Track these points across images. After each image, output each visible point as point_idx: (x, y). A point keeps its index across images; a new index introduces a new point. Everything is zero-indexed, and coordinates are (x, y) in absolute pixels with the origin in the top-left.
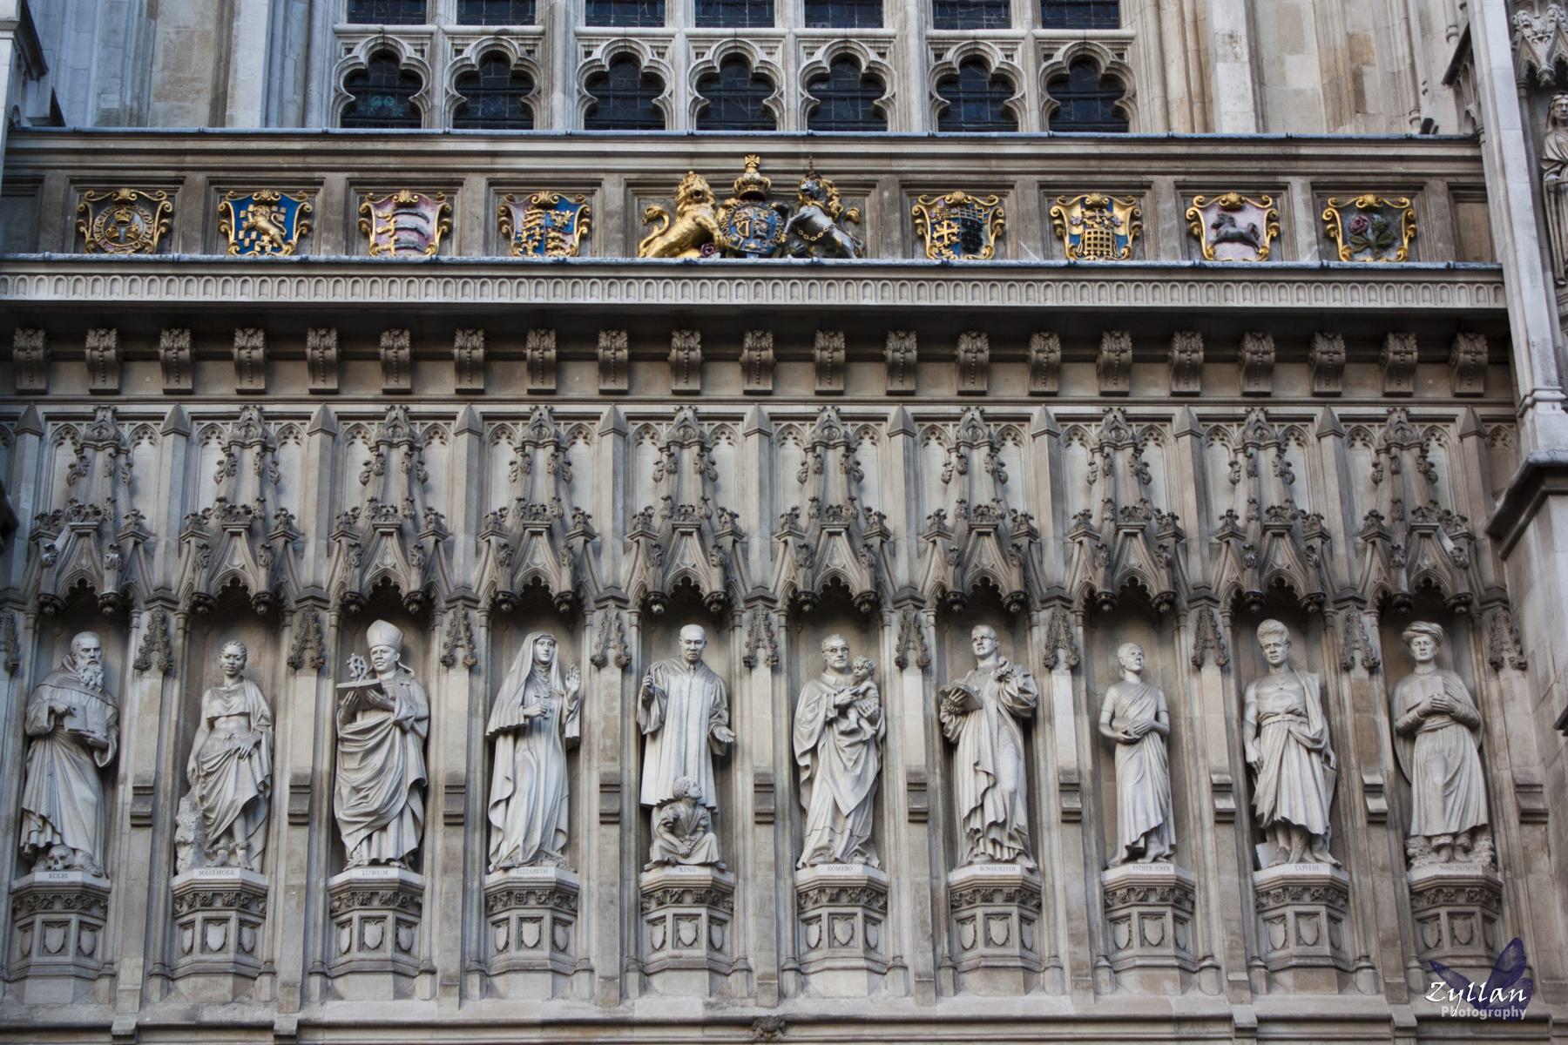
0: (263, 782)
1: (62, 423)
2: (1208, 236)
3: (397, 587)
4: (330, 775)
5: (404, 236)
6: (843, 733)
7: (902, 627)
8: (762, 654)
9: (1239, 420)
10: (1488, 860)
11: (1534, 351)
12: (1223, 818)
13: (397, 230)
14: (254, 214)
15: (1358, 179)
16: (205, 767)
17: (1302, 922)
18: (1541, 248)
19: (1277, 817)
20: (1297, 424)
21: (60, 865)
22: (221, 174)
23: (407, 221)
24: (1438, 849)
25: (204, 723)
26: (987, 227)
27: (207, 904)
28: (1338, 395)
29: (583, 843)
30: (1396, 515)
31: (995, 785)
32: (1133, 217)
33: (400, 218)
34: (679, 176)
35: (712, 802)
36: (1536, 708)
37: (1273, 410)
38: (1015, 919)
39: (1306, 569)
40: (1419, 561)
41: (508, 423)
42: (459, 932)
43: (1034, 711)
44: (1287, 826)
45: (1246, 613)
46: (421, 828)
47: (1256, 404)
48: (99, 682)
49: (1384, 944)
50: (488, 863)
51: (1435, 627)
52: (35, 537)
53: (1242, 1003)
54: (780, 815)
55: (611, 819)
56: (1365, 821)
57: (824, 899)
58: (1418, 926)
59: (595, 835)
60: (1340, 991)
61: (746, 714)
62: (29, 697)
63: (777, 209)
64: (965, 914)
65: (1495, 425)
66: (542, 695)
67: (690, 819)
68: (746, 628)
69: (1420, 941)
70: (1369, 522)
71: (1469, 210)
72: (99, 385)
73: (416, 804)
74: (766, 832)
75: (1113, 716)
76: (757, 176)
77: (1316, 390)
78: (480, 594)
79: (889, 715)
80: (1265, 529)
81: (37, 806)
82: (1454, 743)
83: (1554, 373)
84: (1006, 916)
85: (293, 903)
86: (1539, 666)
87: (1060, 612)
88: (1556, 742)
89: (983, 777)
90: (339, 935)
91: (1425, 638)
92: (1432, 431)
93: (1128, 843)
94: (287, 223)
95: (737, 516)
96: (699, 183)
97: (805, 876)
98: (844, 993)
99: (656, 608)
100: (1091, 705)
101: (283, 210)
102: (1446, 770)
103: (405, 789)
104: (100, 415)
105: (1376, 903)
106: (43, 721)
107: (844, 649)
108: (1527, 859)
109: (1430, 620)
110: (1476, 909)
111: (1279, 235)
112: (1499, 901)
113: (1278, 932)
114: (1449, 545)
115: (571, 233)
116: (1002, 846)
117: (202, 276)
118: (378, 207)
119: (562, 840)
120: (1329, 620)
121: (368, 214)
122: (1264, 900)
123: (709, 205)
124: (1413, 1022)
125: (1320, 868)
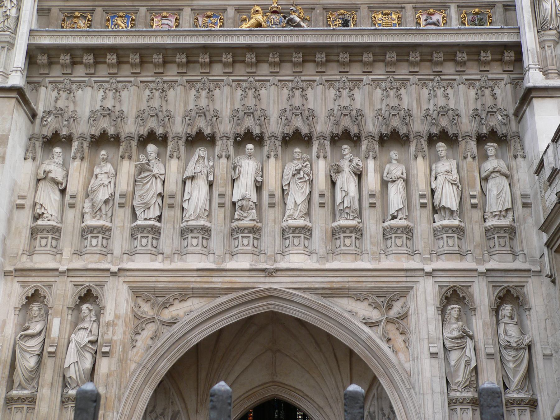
0: (111, 194)
1: (54, 84)
2: (423, 23)
3: (155, 133)
4: (133, 192)
5: (164, 26)
6: (298, 179)
7: (319, 145)
8: (272, 154)
9: (432, 80)
10: (512, 219)
11: (529, 52)
12: (423, 206)
13: (161, 24)
14: (117, 20)
15: (473, 4)
16: (93, 189)
17: (449, 239)
18: (533, 20)
19: (441, 206)
20: (451, 81)
21: (46, 219)
22: (106, 8)
23: (165, 22)
24: (495, 216)
25: (94, 176)
26: (351, 21)
27: (92, 232)
28: (464, 71)
29: (213, 214)
30: (483, 109)
31: (347, 195)
32: (398, 18)
33: (163, 21)
34: (252, 6)
35: (255, 201)
36: (528, 170)
37: (443, 77)
38: (354, 238)
39: (452, 126)
40: (490, 123)
41: (194, 83)
42: (171, 241)
43: (362, 172)
44: (444, 208)
45: (432, 140)
46: (161, 209)
47: (436, 75)
48: (61, 163)
49: (475, 246)
50: (182, 220)
51: (495, 145)
52: (42, 118)
53: (427, 265)
54: (276, 204)
55: (222, 206)
56: (470, 207)
57: (291, 231)
58: (488, 241)
59: (217, 211)
60: (461, 261)
61: (267, 173)
62: (39, 167)
63: (283, 16)
64: (337, 237)
65: (517, 81)
66: (200, 166)
67: (247, 206)
68: (268, 146)
69: (488, 246)
70: (474, 111)
71: (510, 14)
72: (65, 72)
73: (160, 200)
74: (271, 211)
75: (388, 173)
76: (276, 5)
77: (457, 70)
78: (183, 135)
79: (314, 173)
80: (439, 113)
81: (39, 201)
82: (501, 182)
83: (536, 59)
84: (351, 237)
85: (119, 232)
86: (529, 156)
87: (371, 140)
88: (535, 179)
89: (343, 192)
90: (134, 242)
91: (492, 148)
92: (495, 84)
93: (391, 213)
94: (127, 23)
95: (266, 110)
96: (257, 8)
97: (284, 224)
98: (296, 261)
99: (238, 139)
100: (381, 170)
101: (126, 19)
102: (498, 190)
103: (155, 196)
104: (66, 81)
105: (473, 233)
106: (42, 175)
107: (299, 152)
108: (525, 219)
109: (493, 143)
110: (507, 235)
111: (446, 22)
112: (515, 233)
113: (441, 242)
114: (500, 118)
115: (217, 25)
116: (350, 215)
117: (96, 36)
118: (156, 17)
119: (207, 213)
120: (460, 143)
121: (153, 20)
122: (436, 233)
123: (261, 15)
124: (485, 271)
125: (455, 222)
